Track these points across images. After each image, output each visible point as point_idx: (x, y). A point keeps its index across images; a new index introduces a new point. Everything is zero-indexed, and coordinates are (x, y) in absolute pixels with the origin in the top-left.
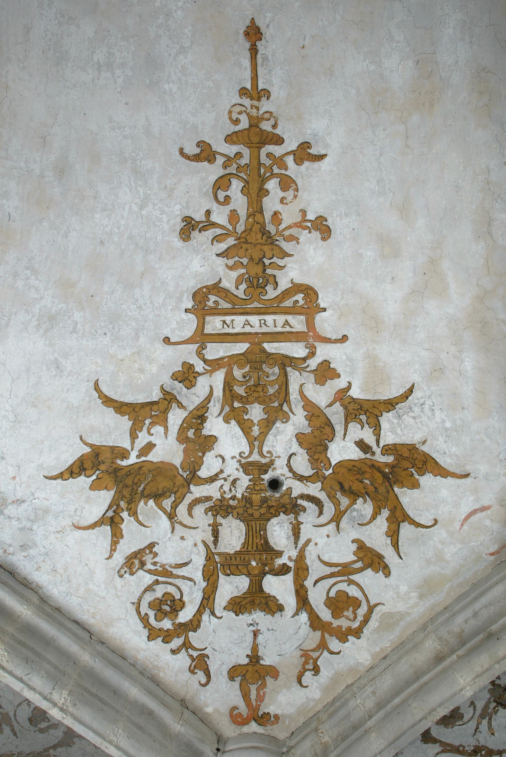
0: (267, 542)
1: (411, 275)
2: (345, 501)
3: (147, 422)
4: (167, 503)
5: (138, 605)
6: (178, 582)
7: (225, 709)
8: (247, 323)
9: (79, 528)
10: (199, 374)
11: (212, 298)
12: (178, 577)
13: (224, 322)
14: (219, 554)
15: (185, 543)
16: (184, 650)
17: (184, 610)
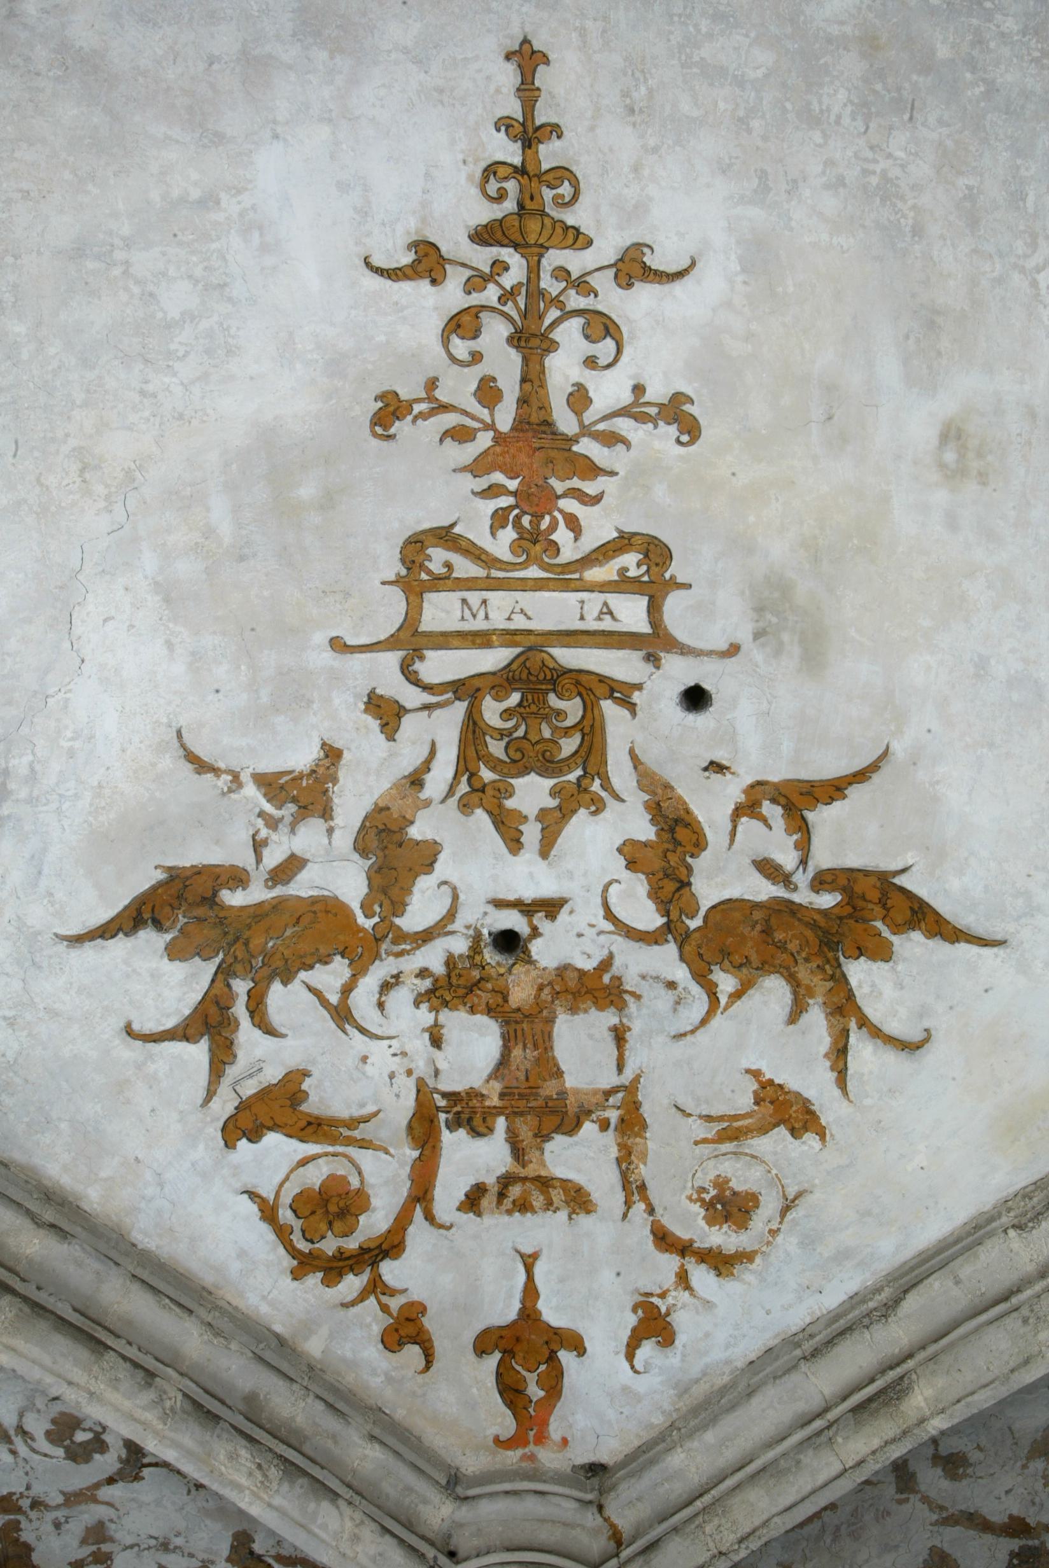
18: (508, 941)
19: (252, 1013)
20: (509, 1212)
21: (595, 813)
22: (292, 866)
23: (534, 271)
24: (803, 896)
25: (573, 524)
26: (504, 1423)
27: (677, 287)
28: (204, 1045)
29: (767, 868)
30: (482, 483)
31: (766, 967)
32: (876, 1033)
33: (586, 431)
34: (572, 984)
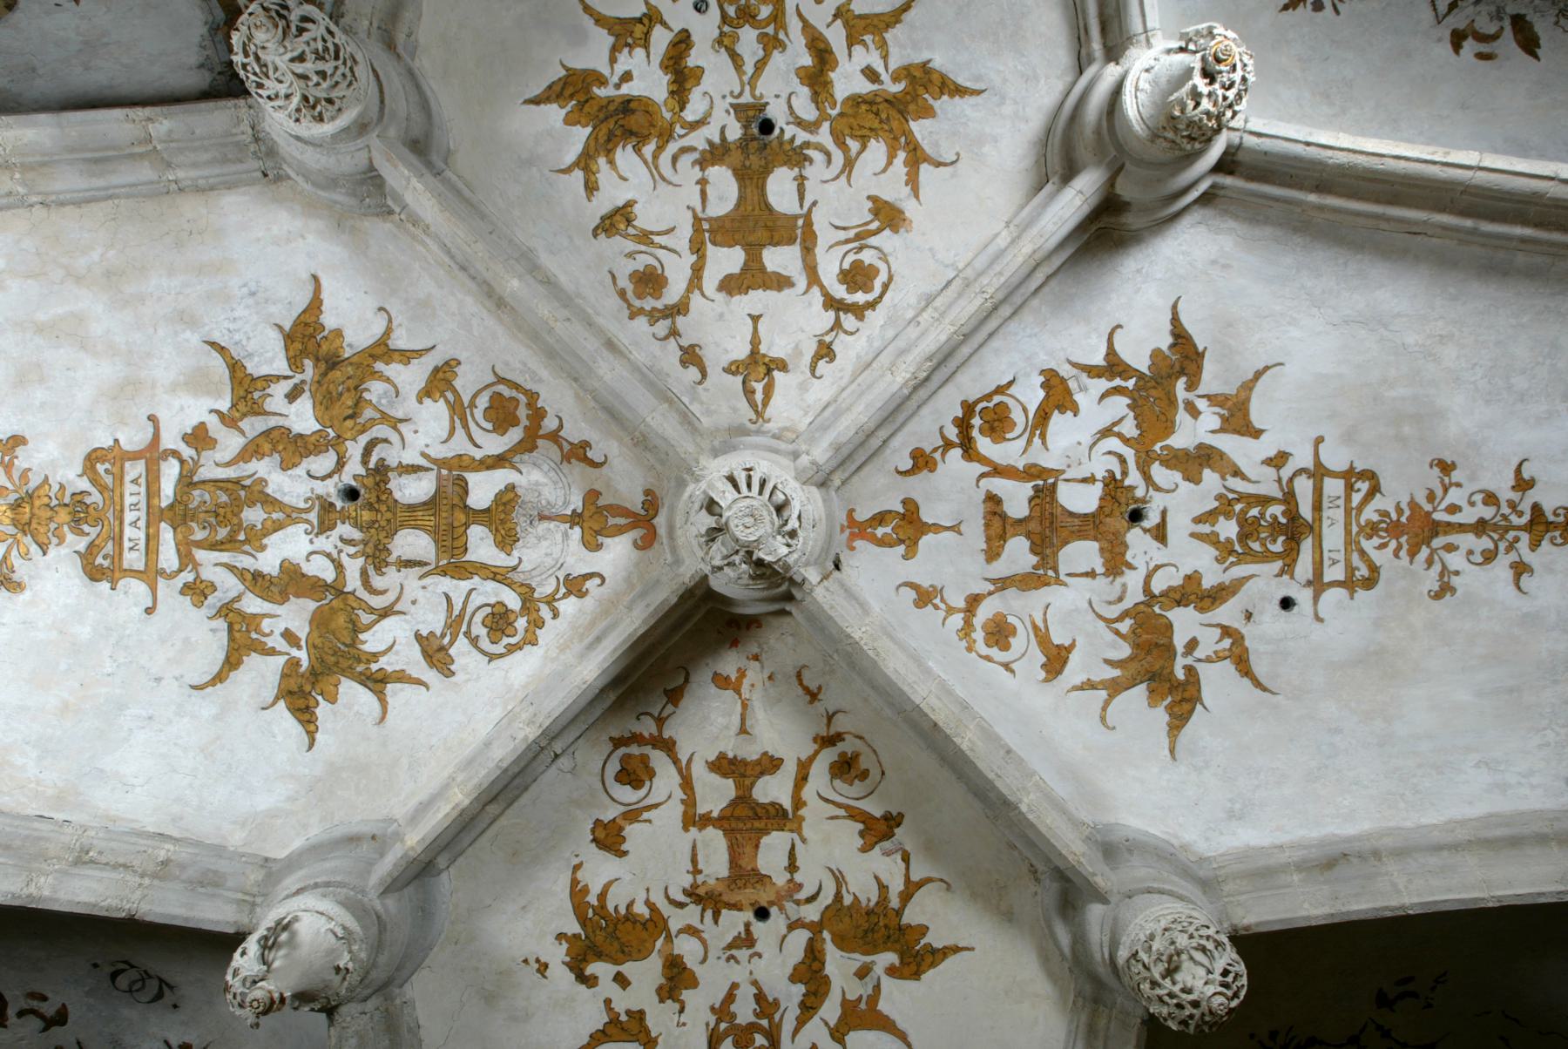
0: (424, 504)
1: (62, 351)
2: (368, 413)
3: (254, 635)
4: (366, 618)
5: (492, 657)
6: (469, 610)
7: (635, 554)
8: (134, 524)
9: (383, 718)
10: (198, 576)
11: (99, 560)
12: (464, 608)
13: (131, 549)
14: (438, 560)
15: (421, 600)
16: (556, 604)
17: (507, 603)
18: (1136, 516)
19: (1115, 388)
20: (984, 518)
21: (1217, 559)
22: (1194, 412)
23: (1519, 528)
24: (1180, 664)
25: (1383, 546)
26: (863, 515)
27: (1512, 588)
28: (1103, 363)
29: (1192, 645)
30: (1404, 506)
31: (1136, 646)
32: (1106, 704)
33: (1433, 551)
34: (1117, 550)
